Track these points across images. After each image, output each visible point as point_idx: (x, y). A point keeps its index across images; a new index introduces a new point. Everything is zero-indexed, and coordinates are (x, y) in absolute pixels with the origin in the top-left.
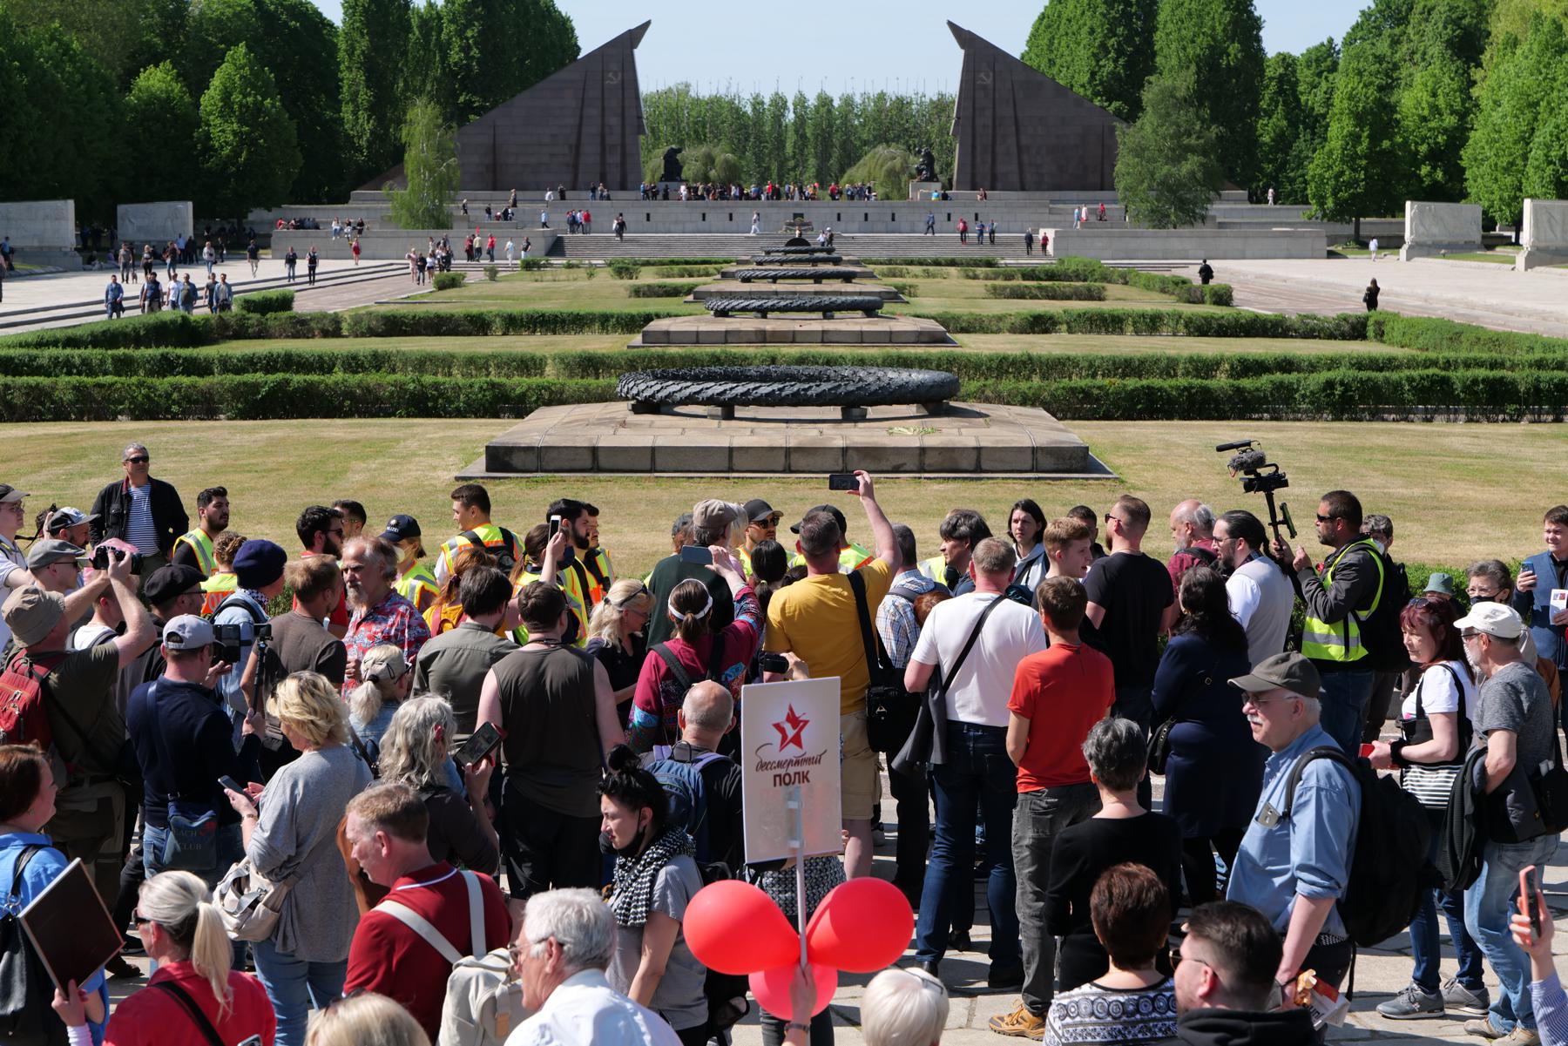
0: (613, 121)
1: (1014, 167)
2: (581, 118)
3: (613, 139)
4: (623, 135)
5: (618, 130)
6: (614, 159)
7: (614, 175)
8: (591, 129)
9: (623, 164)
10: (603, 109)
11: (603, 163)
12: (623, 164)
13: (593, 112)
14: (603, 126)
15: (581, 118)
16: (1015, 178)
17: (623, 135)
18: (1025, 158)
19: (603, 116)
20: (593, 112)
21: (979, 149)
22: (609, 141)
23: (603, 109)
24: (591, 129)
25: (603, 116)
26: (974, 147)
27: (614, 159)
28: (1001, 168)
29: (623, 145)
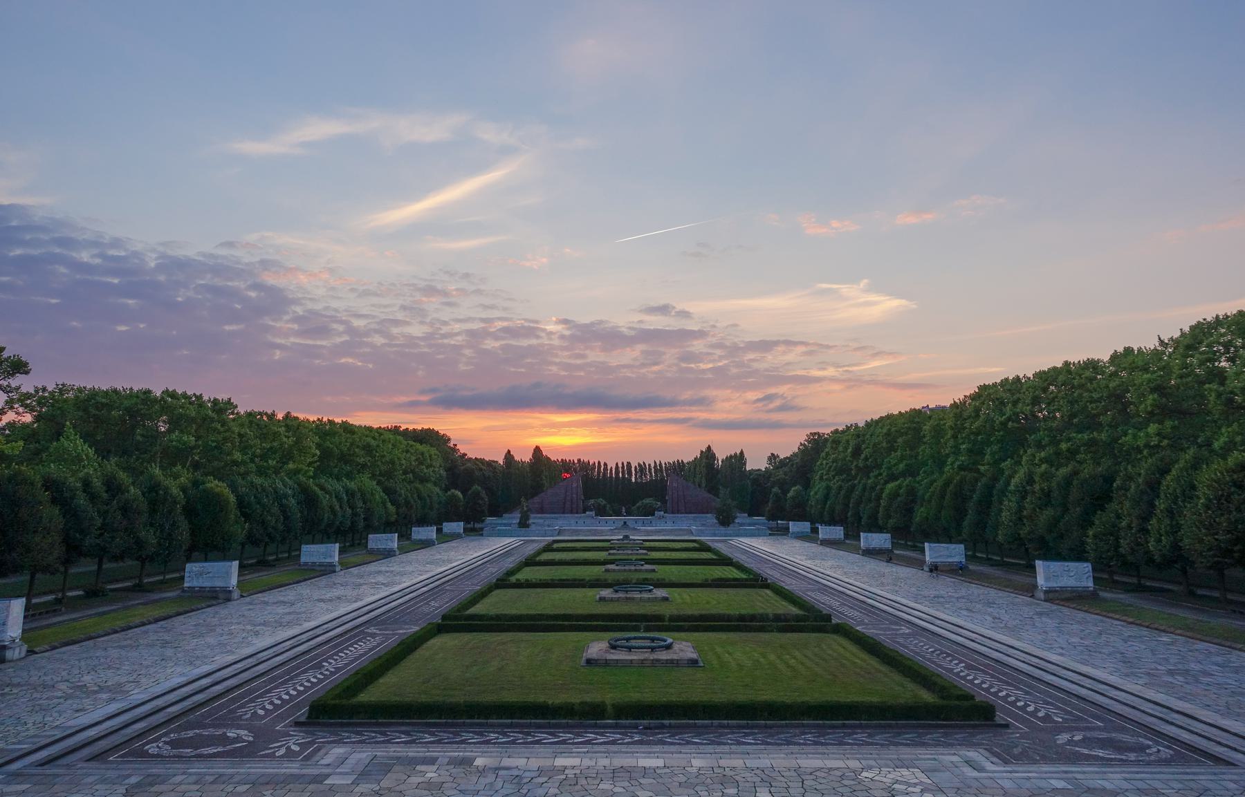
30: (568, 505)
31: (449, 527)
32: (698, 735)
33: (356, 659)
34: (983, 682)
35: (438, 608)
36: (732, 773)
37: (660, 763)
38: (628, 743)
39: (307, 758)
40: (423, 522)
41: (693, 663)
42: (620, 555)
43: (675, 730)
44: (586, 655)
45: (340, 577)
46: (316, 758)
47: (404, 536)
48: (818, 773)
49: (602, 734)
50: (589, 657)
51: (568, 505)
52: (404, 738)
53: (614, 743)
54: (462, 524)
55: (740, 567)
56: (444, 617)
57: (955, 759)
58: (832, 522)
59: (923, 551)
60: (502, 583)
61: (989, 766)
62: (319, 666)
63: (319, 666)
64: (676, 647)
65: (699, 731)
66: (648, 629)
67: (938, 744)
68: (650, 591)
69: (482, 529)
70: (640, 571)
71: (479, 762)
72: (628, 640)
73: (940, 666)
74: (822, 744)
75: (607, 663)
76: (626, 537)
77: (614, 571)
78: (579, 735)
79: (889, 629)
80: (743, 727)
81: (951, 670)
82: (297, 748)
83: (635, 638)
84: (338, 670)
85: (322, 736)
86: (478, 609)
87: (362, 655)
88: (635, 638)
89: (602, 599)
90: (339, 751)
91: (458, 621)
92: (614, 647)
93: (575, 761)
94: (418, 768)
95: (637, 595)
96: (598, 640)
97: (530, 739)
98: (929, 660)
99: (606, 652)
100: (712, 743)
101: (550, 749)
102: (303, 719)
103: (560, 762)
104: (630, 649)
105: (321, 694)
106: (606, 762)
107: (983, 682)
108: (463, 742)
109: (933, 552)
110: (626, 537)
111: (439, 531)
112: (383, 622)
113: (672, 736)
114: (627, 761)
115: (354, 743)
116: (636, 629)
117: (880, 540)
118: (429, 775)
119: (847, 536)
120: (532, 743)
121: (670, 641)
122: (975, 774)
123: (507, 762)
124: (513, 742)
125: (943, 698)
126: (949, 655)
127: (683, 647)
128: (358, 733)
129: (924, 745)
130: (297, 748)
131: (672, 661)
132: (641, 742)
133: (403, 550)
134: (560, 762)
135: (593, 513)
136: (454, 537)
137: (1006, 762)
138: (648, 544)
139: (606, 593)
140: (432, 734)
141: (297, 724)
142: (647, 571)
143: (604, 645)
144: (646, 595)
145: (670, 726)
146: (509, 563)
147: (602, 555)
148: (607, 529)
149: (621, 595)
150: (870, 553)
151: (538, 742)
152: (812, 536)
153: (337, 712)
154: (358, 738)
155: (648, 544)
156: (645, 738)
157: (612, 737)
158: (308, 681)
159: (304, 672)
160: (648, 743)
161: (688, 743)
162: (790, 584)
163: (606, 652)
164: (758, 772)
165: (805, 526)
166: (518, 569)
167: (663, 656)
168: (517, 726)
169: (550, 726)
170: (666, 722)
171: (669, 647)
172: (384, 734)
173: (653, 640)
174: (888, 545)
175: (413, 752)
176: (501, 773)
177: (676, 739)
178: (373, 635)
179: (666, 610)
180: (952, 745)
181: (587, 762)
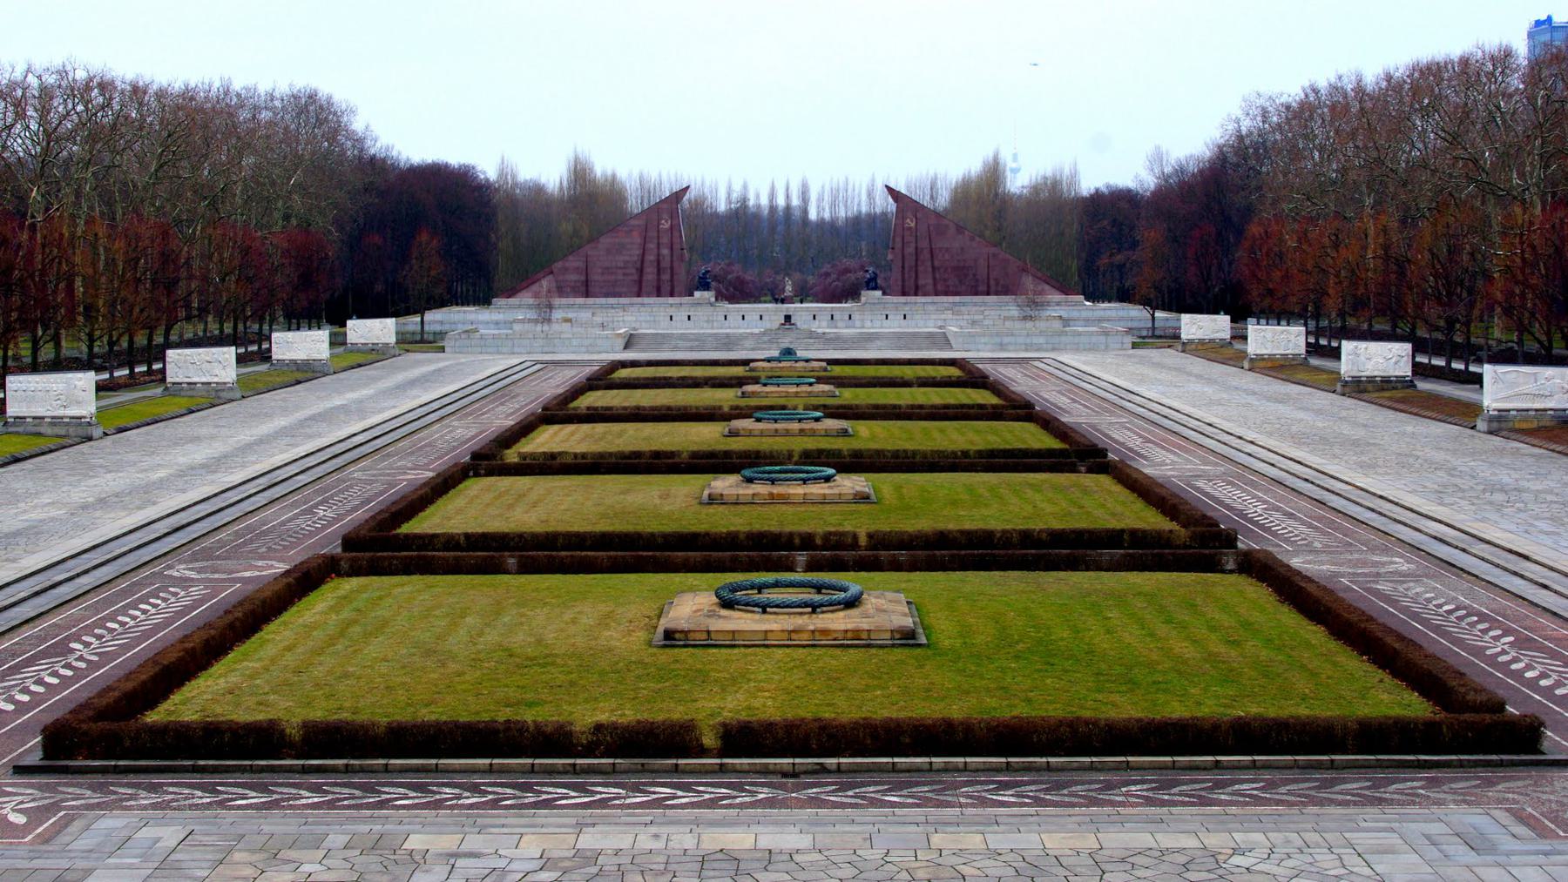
0: (665, 252)
3: (666, 263)
5: (668, 259)
6: (666, 277)
7: (666, 287)
9: (672, 281)
11: (659, 280)
12: (672, 281)
16: (930, 288)
22: (663, 265)
27: (666, 277)
29: (672, 268)
30: (650, 274)
31: (362, 330)
32: (896, 787)
33: (146, 635)
34: (1543, 676)
35: (326, 522)
36: (954, 860)
37: (804, 841)
38: (742, 806)
39: (46, 839)
40: (300, 317)
41: (906, 638)
42: (770, 393)
43: (847, 779)
44: (664, 624)
45: (102, 450)
46: (63, 838)
47: (255, 354)
48: (1138, 860)
49: (687, 788)
50: (672, 625)
51: (650, 274)
52: (256, 798)
53: (713, 804)
54: (390, 322)
55: (1048, 423)
56: (350, 542)
57: (1435, 828)
58: (1278, 313)
59: (1477, 380)
60: (488, 460)
61: (1508, 843)
62: (62, 649)
63: (62, 649)
64: (871, 602)
65: (901, 780)
66: (812, 567)
67: (1412, 799)
68: (828, 479)
69: (441, 335)
70: (813, 433)
71: (415, 842)
72: (760, 588)
73: (1459, 642)
74: (1163, 803)
75: (709, 641)
76: (788, 352)
77: (750, 434)
78: (637, 789)
79: (1364, 564)
80: (997, 770)
81: (1479, 652)
82: (20, 819)
83: (777, 585)
84: (105, 657)
85: (76, 793)
86: (427, 523)
87: (157, 628)
88: (777, 585)
89: (713, 500)
90: (112, 823)
91: (385, 545)
92: (727, 604)
93: (625, 842)
94: (286, 854)
95: (797, 490)
96: (693, 589)
97: (530, 798)
98: (1437, 629)
99: (711, 614)
100: (924, 802)
101: (570, 818)
102: (35, 759)
103: (589, 840)
104: (764, 607)
105: (85, 695)
106: (689, 842)
107: (1543, 676)
108: (382, 805)
109: (1506, 387)
110: (788, 352)
111: (337, 341)
112: (207, 554)
113: (843, 788)
114: (739, 839)
115: (145, 808)
116: (791, 568)
117: (1384, 358)
118: (306, 868)
119: (1313, 350)
120: (535, 805)
121: (854, 589)
122: (1472, 858)
123: (474, 842)
124: (494, 804)
125: (1445, 708)
126: (1483, 617)
127: (885, 603)
128: (153, 788)
129: (1380, 801)
130: (20, 819)
131: (856, 634)
132: (770, 803)
133: (248, 389)
134: (589, 840)
135: (709, 295)
136: (374, 355)
137: (1543, 833)
138: (837, 370)
139: (725, 484)
140: (317, 789)
141: (20, 770)
142: (827, 434)
143: (707, 600)
144: (817, 489)
145: (839, 770)
146: (503, 418)
147: (725, 397)
148: (745, 329)
149: (761, 489)
150: (1360, 388)
151: (547, 804)
152: (1226, 353)
153: (116, 736)
154: (154, 798)
155: (837, 370)
156: (781, 794)
157: (709, 793)
158: (40, 682)
159: (30, 662)
160: (784, 804)
161: (874, 803)
162: (1161, 465)
163: (711, 614)
164: (1010, 857)
165: (1216, 326)
166: (525, 428)
167: (839, 621)
168: (503, 771)
169: (575, 770)
170: (831, 761)
171: (852, 603)
172: (212, 790)
173: (819, 588)
174: (1406, 370)
175: (278, 825)
176: (460, 863)
177: (848, 797)
178: (184, 582)
179: (861, 524)
180: (1439, 803)
181: (645, 842)
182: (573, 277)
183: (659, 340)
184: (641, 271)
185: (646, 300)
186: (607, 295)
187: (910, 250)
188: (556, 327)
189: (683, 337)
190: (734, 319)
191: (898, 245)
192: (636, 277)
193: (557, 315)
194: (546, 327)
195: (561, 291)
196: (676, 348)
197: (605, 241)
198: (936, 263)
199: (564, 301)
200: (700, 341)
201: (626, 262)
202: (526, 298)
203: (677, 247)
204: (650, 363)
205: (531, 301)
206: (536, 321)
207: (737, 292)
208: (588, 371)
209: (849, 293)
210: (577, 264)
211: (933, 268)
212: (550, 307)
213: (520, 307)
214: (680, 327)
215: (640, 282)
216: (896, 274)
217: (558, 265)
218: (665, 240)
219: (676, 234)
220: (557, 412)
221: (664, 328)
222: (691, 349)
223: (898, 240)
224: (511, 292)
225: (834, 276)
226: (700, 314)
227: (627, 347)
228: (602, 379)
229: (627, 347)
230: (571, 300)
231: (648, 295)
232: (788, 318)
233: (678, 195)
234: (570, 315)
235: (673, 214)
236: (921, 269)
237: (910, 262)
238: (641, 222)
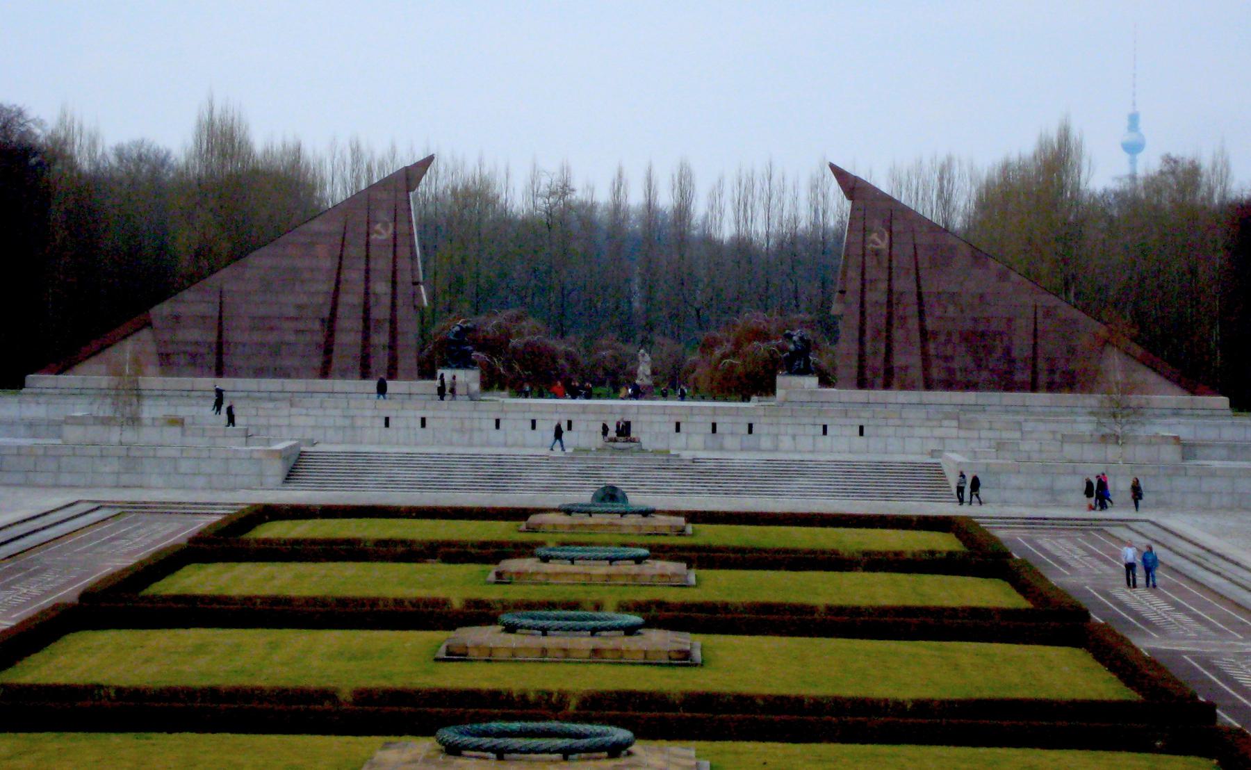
1: (916, 361)
2: (338, 282)
3: (381, 312)
4: (394, 307)
5: (387, 300)
6: (380, 338)
7: (380, 361)
8: (351, 298)
10: (367, 271)
13: (354, 276)
14: (367, 293)
15: (338, 282)
17: (394, 307)
18: (932, 347)
19: (367, 280)
20: (354, 276)
21: (868, 332)
23: (367, 271)
24: (351, 298)
25: (367, 280)
26: (862, 331)
27: (380, 338)
28: (898, 360)
29: (393, 321)
135: (468, 378)
182: (195, 334)
183: (357, 465)
184: (330, 324)
185: (338, 384)
186: (259, 373)
187: (877, 295)
188: (148, 435)
189: (407, 460)
190: (516, 426)
191: (855, 285)
192: (320, 338)
193: (151, 410)
194: (129, 435)
195: (167, 361)
196: (392, 483)
197: (259, 262)
198: (930, 324)
199: (172, 382)
200: (441, 470)
201: (300, 307)
202: (92, 375)
203: (404, 278)
204: (329, 512)
205: (105, 381)
206: (105, 422)
207: (525, 371)
208: (201, 523)
209: (754, 383)
210: (202, 309)
211: (925, 335)
212: (138, 394)
213: (80, 392)
214: (404, 439)
215: (328, 349)
216: (847, 343)
217: (162, 310)
218: (382, 264)
219: (403, 251)
220: (122, 602)
221: (372, 441)
222: (423, 485)
223: (854, 274)
224: (63, 361)
225: (727, 347)
226: (445, 414)
227: (290, 476)
228: (230, 539)
229: (290, 476)
230: (186, 382)
231: (344, 374)
232: (624, 430)
233: (412, 175)
234: (183, 412)
235: (399, 212)
236: (898, 334)
237: (876, 318)
238: (336, 227)
